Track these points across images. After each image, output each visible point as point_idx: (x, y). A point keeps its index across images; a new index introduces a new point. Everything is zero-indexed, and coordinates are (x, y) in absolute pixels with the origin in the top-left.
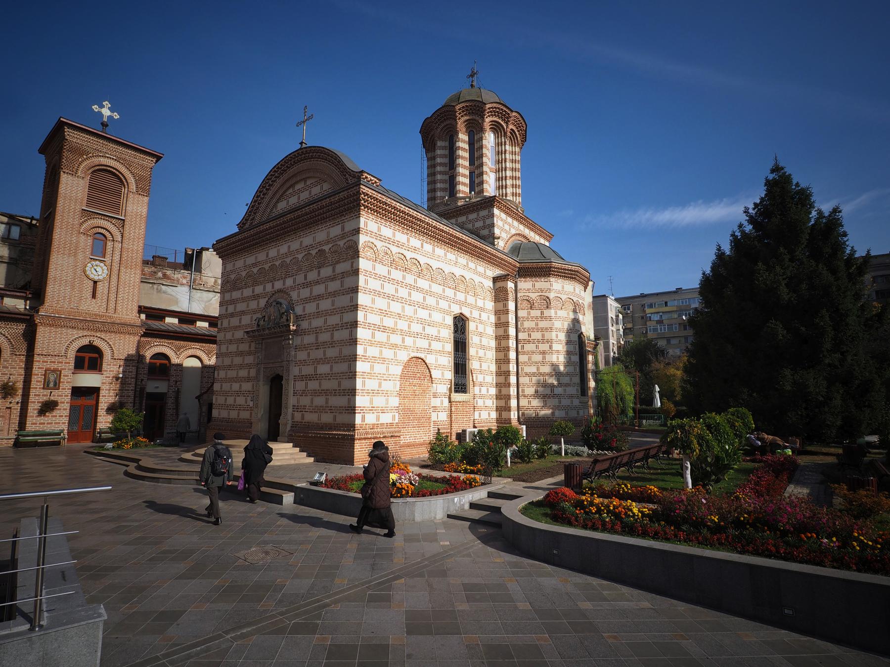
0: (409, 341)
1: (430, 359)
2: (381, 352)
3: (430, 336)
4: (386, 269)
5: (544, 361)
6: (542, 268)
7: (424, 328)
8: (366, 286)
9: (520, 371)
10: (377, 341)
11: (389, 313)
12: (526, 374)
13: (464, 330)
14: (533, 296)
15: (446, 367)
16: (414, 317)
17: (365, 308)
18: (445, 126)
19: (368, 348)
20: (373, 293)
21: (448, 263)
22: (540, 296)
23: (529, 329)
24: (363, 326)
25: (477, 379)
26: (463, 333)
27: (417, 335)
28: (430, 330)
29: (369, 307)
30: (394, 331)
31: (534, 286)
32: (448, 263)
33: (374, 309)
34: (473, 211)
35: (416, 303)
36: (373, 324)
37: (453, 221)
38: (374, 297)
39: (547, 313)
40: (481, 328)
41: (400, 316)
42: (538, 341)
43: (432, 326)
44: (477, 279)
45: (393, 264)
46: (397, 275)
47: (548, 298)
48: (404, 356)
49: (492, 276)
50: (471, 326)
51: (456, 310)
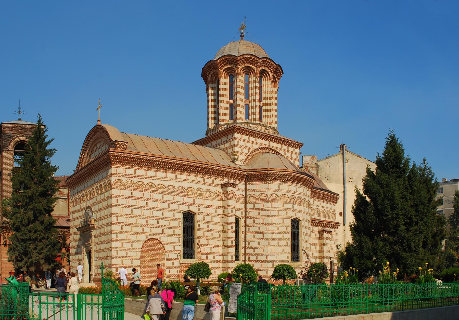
0: (147, 230)
1: (163, 239)
2: (127, 237)
3: (164, 226)
4: (130, 192)
5: (263, 238)
6: (262, 175)
7: (158, 222)
8: (117, 203)
9: (247, 245)
10: (125, 231)
11: (132, 216)
12: (252, 247)
13: (192, 221)
14: (257, 194)
15: (177, 243)
16: (150, 216)
17: (116, 215)
18: (213, 73)
19: (119, 235)
20: (121, 206)
21: (177, 181)
22: (262, 194)
23: (254, 217)
24: (115, 224)
25: (204, 249)
26: (192, 223)
27: (153, 226)
28: (161, 223)
29: (119, 214)
30: (136, 225)
31: (258, 187)
32: (177, 181)
33: (122, 215)
34: (224, 136)
35: (152, 208)
36: (122, 223)
37: (209, 144)
38: (122, 208)
39: (266, 205)
40: (208, 218)
41: (140, 216)
42: (259, 225)
43: (165, 220)
44: (204, 187)
45: (138, 187)
46: (137, 194)
47: (267, 195)
48: (143, 238)
49: (220, 184)
50: (198, 218)
51: (185, 208)
